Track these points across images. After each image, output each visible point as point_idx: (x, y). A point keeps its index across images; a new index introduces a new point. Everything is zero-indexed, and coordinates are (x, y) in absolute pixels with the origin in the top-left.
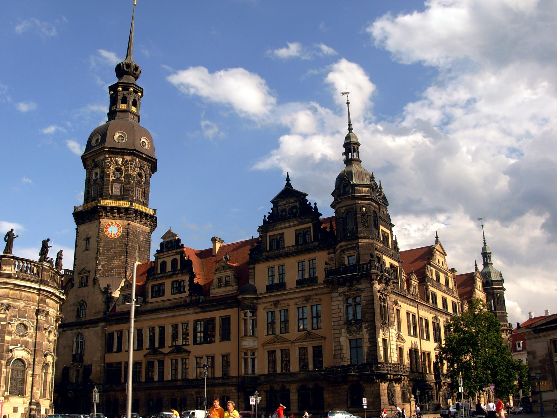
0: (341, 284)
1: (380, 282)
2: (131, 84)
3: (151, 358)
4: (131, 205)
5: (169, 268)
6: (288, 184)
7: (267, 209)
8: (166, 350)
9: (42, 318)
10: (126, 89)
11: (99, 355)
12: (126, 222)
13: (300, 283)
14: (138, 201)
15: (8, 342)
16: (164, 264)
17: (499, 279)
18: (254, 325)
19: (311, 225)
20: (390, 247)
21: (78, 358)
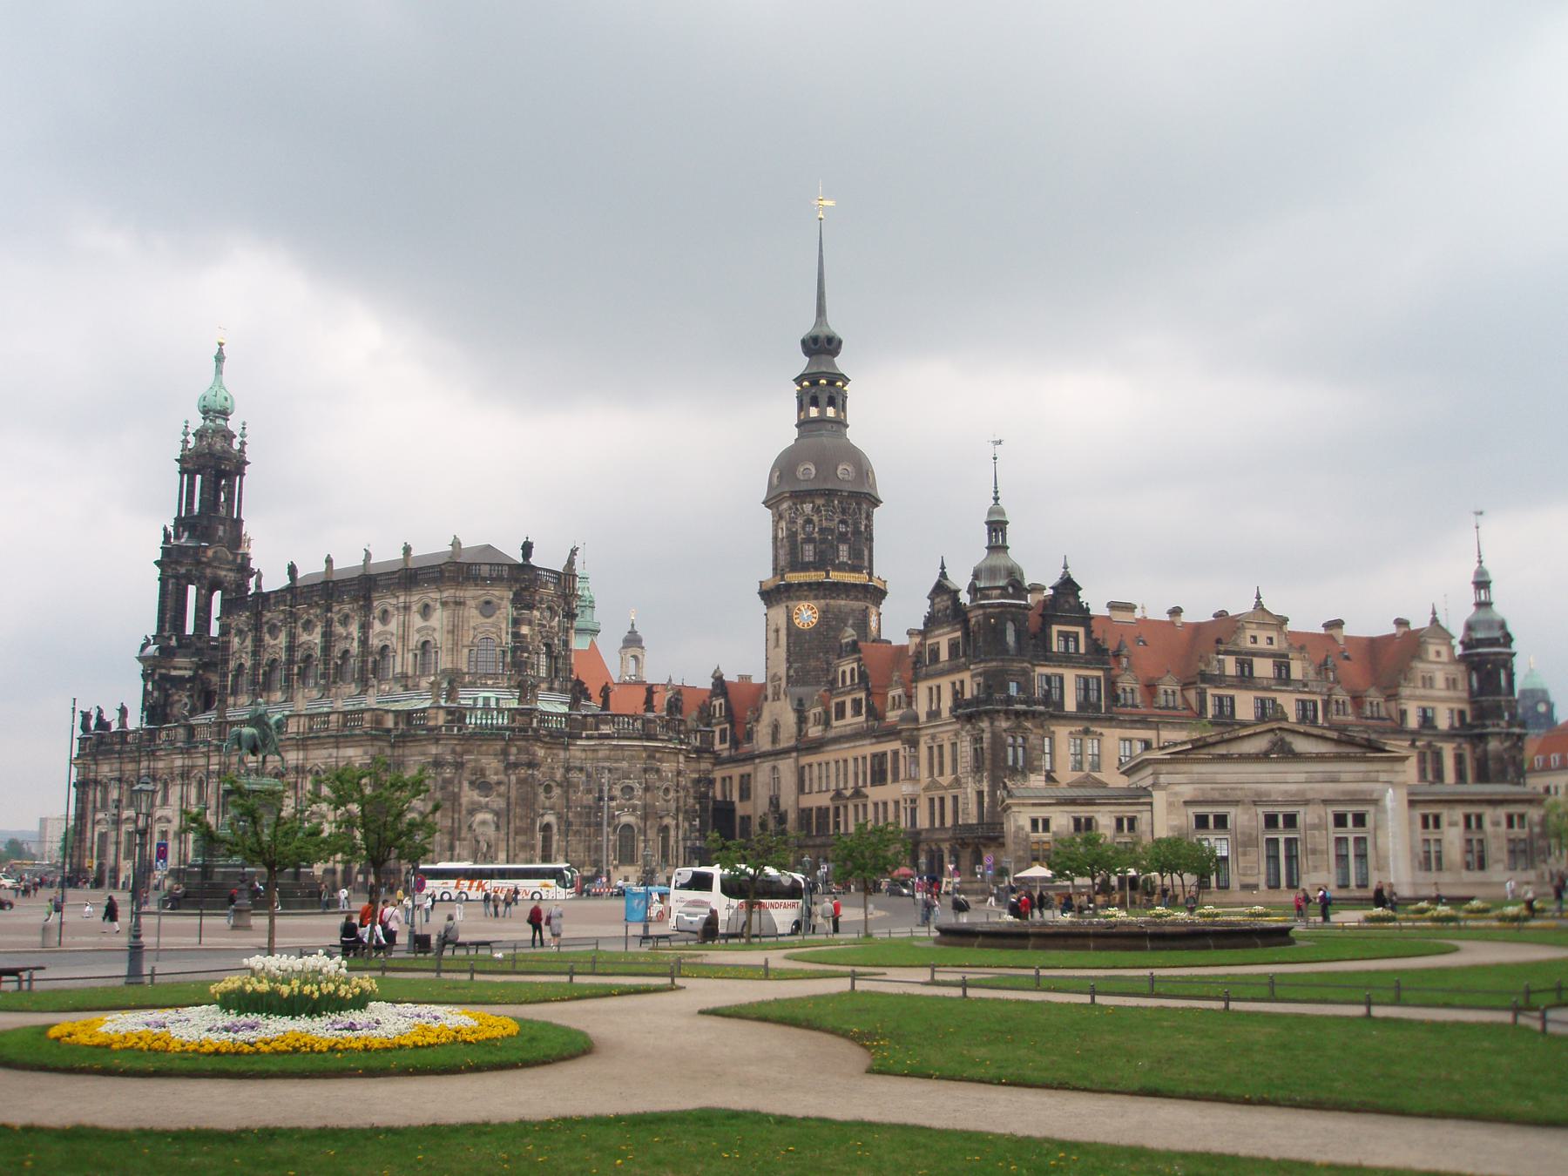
0: (969, 718)
1: (1008, 719)
2: (823, 375)
3: (838, 803)
5: (848, 682)
6: (943, 575)
7: (924, 607)
8: (848, 793)
9: (652, 776)
10: (814, 383)
11: (793, 797)
13: (952, 710)
14: (841, 567)
17: (1497, 634)
18: (918, 765)
19: (959, 634)
20: (1082, 650)
21: (774, 802)
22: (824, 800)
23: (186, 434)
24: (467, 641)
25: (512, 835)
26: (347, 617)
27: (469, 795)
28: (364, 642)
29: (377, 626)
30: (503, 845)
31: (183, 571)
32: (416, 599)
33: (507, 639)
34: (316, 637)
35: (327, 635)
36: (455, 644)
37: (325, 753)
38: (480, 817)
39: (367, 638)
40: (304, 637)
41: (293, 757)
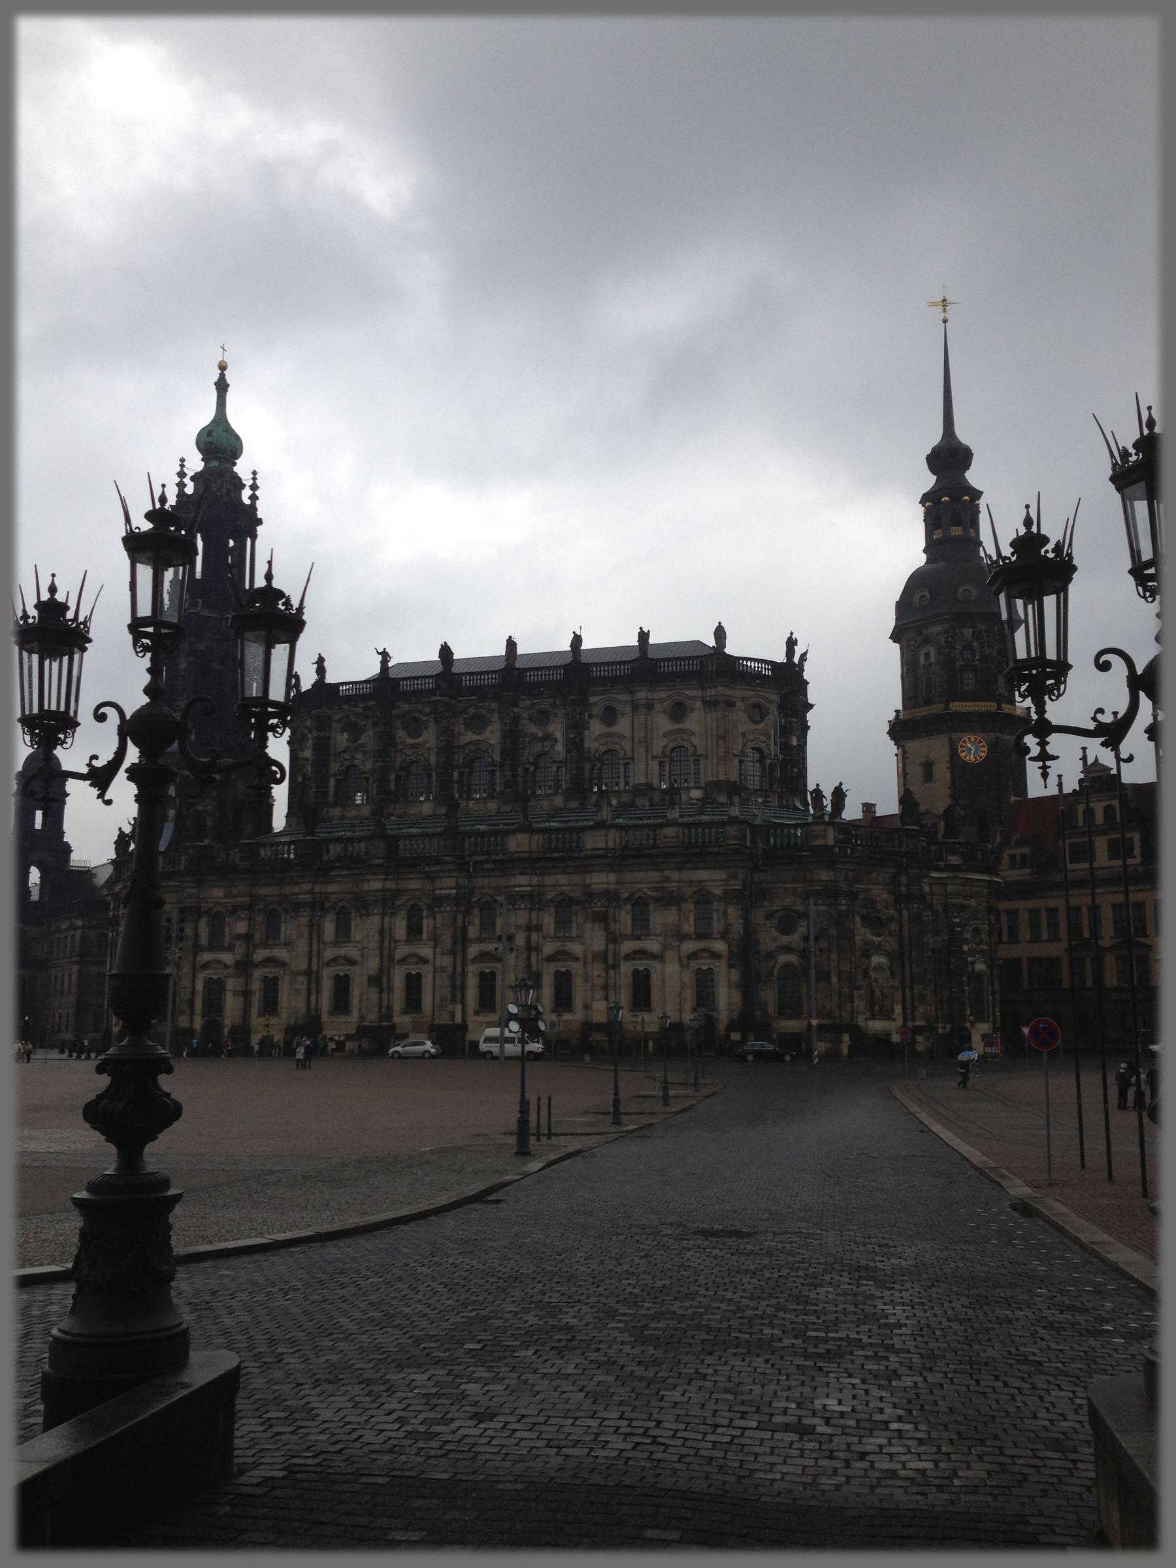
4: (999, 708)
5: (1099, 818)
10: (956, 499)
12: (992, 735)
15: (965, 952)
16: (1089, 813)
22: (1057, 949)
23: (182, 474)
24: (737, 748)
25: (908, 983)
26: (543, 712)
27: (863, 933)
28: (575, 745)
29: (596, 727)
30: (898, 995)
31: (201, 646)
32: (663, 695)
33: (774, 749)
34: (492, 735)
35: (512, 735)
36: (727, 752)
37: (654, 875)
38: (876, 960)
39: (582, 740)
40: (469, 737)
41: (601, 880)
